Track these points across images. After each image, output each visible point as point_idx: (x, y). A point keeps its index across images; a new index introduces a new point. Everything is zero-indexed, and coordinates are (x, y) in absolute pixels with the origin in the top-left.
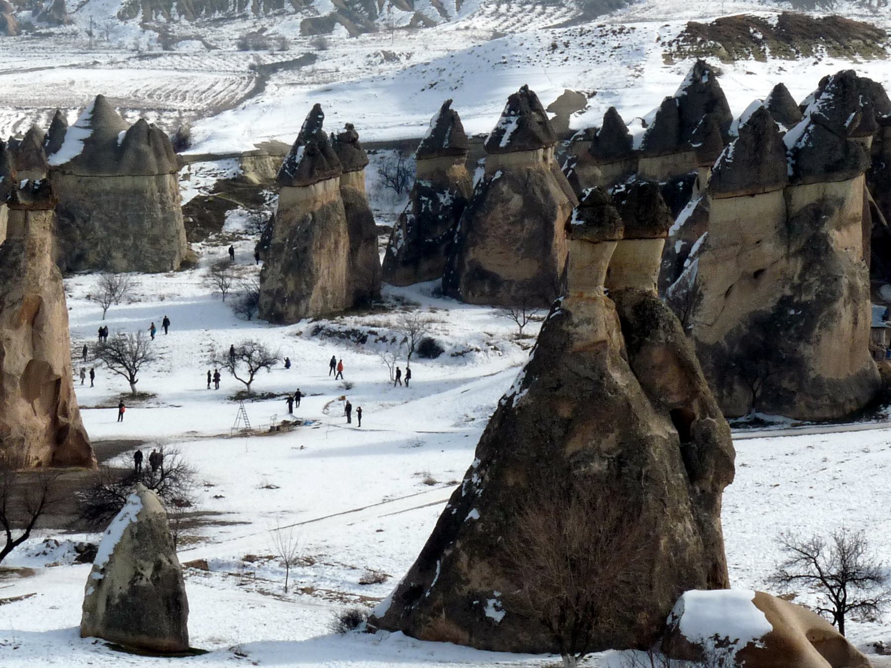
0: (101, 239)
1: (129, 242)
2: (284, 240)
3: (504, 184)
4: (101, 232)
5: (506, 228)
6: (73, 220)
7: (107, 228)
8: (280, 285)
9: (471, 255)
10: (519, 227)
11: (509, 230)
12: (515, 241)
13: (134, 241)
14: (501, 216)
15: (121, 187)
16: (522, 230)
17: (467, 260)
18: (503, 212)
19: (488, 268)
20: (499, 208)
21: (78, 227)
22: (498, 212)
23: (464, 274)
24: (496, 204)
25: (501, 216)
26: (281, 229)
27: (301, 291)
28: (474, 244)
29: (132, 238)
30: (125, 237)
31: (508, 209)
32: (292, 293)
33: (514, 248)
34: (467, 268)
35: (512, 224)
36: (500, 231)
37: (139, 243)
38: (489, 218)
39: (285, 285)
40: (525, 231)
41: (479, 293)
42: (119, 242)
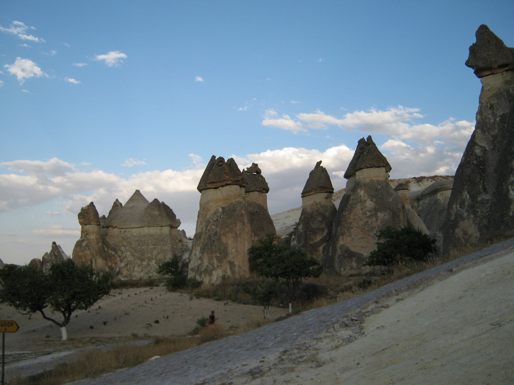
0: (130, 261)
1: (145, 263)
2: (202, 229)
3: (361, 190)
4: (130, 258)
5: (365, 220)
6: (116, 252)
7: (133, 256)
8: (199, 262)
9: (341, 242)
10: (374, 219)
11: (368, 222)
12: (373, 228)
13: (148, 262)
14: (361, 212)
15: (142, 234)
16: (377, 220)
17: (338, 246)
18: (362, 209)
19: (353, 249)
20: (359, 206)
21: (118, 256)
22: (358, 209)
23: (337, 256)
24: (357, 204)
25: (361, 212)
26: (201, 222)
27: (213, 265)
28: (343, 234)
29: (146, 260)
30: (142, 260)
31: (365, 207)
32: (207, 266)
33: (372, 234)
34: (339, 252)
35: (369, 217)
37: (150, 263)
38: (352, 214)
39: (202, 261)
40: (379, 221)
41: (349, 268)
42: (140, 263)
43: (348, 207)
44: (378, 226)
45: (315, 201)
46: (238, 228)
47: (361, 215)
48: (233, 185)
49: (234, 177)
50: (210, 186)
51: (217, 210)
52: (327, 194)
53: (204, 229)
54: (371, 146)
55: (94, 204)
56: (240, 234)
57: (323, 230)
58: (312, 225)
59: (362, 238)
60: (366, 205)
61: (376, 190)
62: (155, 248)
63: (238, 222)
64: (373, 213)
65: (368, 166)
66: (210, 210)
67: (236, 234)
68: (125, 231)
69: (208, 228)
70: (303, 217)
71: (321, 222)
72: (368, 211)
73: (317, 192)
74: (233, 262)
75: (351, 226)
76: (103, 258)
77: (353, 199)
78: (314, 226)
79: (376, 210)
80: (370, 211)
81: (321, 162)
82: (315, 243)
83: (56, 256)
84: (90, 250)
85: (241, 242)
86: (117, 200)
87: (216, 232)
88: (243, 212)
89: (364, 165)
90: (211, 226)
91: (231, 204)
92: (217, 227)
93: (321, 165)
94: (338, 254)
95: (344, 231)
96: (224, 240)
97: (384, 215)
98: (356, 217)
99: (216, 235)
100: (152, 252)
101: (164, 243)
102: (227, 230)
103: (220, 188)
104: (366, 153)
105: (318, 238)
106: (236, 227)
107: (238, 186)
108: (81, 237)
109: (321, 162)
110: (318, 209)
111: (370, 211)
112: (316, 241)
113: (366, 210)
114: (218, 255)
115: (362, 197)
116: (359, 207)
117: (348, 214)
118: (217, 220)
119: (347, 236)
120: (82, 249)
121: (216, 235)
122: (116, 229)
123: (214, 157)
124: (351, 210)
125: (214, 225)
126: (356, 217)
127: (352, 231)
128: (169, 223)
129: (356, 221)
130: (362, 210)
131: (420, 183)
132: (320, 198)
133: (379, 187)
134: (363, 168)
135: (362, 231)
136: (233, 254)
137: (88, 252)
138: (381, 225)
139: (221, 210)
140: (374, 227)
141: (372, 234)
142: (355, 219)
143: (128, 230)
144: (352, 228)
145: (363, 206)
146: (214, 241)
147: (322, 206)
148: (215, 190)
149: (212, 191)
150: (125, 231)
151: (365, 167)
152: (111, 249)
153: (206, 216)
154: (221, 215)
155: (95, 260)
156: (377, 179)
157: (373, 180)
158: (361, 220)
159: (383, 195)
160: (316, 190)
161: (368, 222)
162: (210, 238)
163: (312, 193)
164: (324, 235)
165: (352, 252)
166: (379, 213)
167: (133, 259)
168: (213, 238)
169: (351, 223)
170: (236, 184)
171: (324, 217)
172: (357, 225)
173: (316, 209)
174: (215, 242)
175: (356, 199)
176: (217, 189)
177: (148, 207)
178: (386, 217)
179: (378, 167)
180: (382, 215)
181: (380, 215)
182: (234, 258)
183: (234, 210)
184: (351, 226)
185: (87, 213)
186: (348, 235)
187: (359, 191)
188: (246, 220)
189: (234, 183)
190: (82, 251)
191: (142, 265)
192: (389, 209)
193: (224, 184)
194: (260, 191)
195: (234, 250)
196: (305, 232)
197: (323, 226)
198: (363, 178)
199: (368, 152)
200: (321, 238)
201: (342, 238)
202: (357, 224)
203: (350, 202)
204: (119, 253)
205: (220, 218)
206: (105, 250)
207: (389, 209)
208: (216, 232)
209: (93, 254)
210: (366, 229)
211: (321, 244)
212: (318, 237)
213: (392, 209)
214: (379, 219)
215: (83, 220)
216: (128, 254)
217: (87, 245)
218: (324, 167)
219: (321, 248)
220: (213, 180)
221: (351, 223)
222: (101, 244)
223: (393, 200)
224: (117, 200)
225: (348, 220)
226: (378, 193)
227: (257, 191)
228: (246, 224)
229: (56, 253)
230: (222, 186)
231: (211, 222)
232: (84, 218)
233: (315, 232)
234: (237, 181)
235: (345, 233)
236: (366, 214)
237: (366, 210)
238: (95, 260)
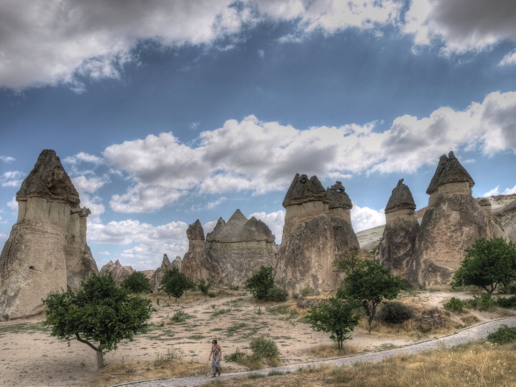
0: (230, 272)
1: (243, 274)
2: (287, 244)
4: (231, 269)
5: (449, 234)
7: (233, 267)
8: (284, 275)
9: (425, 257)
10: (459, 234)
12: (458, 243)
13: (246, 273)
16: (462, 235)
17: (422, 260)
18: (446, 224)
19: (438, 264)
20: (442, 221)
23: (421, 270)
24: (440, 219)
25: (444, 226)
27: (296, 278)
28: (427, 248)
29: (245, 271)
30: (241, 271)
31: (449, 222)
32: (291, 279)
33: (457, 249)
34: (423, 266)
35: (453, 231)
36: (445, 238)
38: (436, 229)
39: (286, 274)
40: (464, 235)
41: (433, 282)
43: (432, 222)
44: (463, 240)
45: (398, 217)
46: (321, 242)
47: (444, 230)
48: (316, 201)
49: (317, 194)
50: (293, 202)
51: (301, 225)
52: (409, 210)
53: (288, 243)
54: (453, 161)
55: (200, 221)
56: (323, 248)
57: (406, 245)
58: (395, 240)
59: (447, 253)
60: (450, 220)
61: (460, 204)
62: (252, 261)
63: (321, 237)
64: (458, 227)
65: (451, 180)
66: (293, 225)
67: (319, 248)
68: (226, 245)
69: (292, 242)
70: (386, 232)
71: (404, 237)
72: (452, 225)
73: (400, 208)
74: (316, 276)
75: (435, 240)
76: (207, 268)
77: (436, 214)
78: (398, 240)
79: (460, 225)
80: (455, 226)
81: (403, 180)
82: (399, 257)
83: (166, 266)
84: (196, 261)
85: (324, 256)
86: (221, 218)
87: (300, 246)
88: (326, 227)
89: (447, 180)
90: (295, 240)
91: (314, 219)
92: (300, 240)
93: (403, 183)
94: (422, 268)
95: (428, 246)
96: (307, 254)
97: (470, 229)
98: (440, 232)
99: (300, 249)
100: (250, 263)
101: (260, 256)
102: (310, 244)
103: (304, 203)
104: (448, 168)
105: (402, 253)
106: (319, 241)
107: (322, 202)
108: (189, 250)
109: (403, 180)
110: (401, 225)
111: (455, 226)
112: (399, 255)
113: (450, 224)
114: (301, 268)
115: (446, 212)
116: (443, 222)
117: (432, 228)
118: (300, 234)
119: (431, 250)
120: (189, 260)
121: (300, 249)
122: (218, 244)
123: (298, 175)
124: (434, 225)
125: (298, 240)
126: (440, 232)
127: (436, 245)
128: (265, 237)
129: (440, 235)
130: (446, 224)
131: (499, 201)
132: (402, 215)
133: (463, 201)
134: (445, 183)
135: (446, 245)
136: (316, 268)
137: (194, 263)
138: (466, 239)
139: (304, 224)
140: (459, 242)
141: (457, 249)
142: (439, 233)
143: (229, 244)
144: (436, 242)
145: (447, 220)
146: (297, 255)
147: (405, 222)
148: (299, 206)
149: (296, 207)
150: (226, 245)
151: (448, 181)
152: (215, 261)
153: (290, 231)
154: (304, 230)
155: (200, 270)
156: (461, 193)
157: (457, 195)
158: (445, 234)
159: (467, 209)
160: (399, 206)
161: (452, 236)
162: (294, 252)
163: (395, 209)
164: (408, 249)
165: (436, 267)
166: (464, 228)
167: (232, 269)
168: (296, 252)
169: (435, 238)
170: (319, 200)
171: (407, 232)
172: (441, 240)
173: (399, 225)
174: (299, 256)
175: (439, 214)
176: (301, 205)
177: (247, 224)
178: (472, 231)
179: (461, 182)
180: (468, 229)
181: (466, 229)
182: (317, 271)
183: (317, 225)
184: (435, 240)
185: (193, 229)
186: (432, 249)
187: (442, 205)
188: (328, 234)
189: (318, 199)
190: (189, 262)
191: (240, 275)
192: (475, 223)
193: (307, 200)
194: (344, 208)
195: (316, 264)
196: (389, 247)
197: (407, 241)
198: (446, 193)
199: (451, 167)
200: (404, 252)
201: (426, 252)
202: (441, 238)
203: (434, 217)
204: (221, 264)
205: (304, 232)
206: (209, 261)
207: (475, 223)
208: (300, 246)
209: (198, 265)
210: (451, 243)
211: (404, 259)
212: (401, 251)
213: (478, 223)
214: (464, 233)
215: (190, 235)
216: (229, 265)
217: (193, 257)
218: (406, 185)
219: (404, 262)
220: (297, 196)
221: (435, 238)
222: (205, 256)
223: (478, 214)
224: (221, 218)
225: (432, 235)
226: (463, 207)
227: (340, 207)
228: (329, 238)
229: (166, 264)
230: (305, 202)
231: (294, 236)
232: (191, 233)
233: (398, 247)
234: (320, 197)
235: (429, 248)
236: (451, 228)
237: (450, 224)
238: (200, 270)
